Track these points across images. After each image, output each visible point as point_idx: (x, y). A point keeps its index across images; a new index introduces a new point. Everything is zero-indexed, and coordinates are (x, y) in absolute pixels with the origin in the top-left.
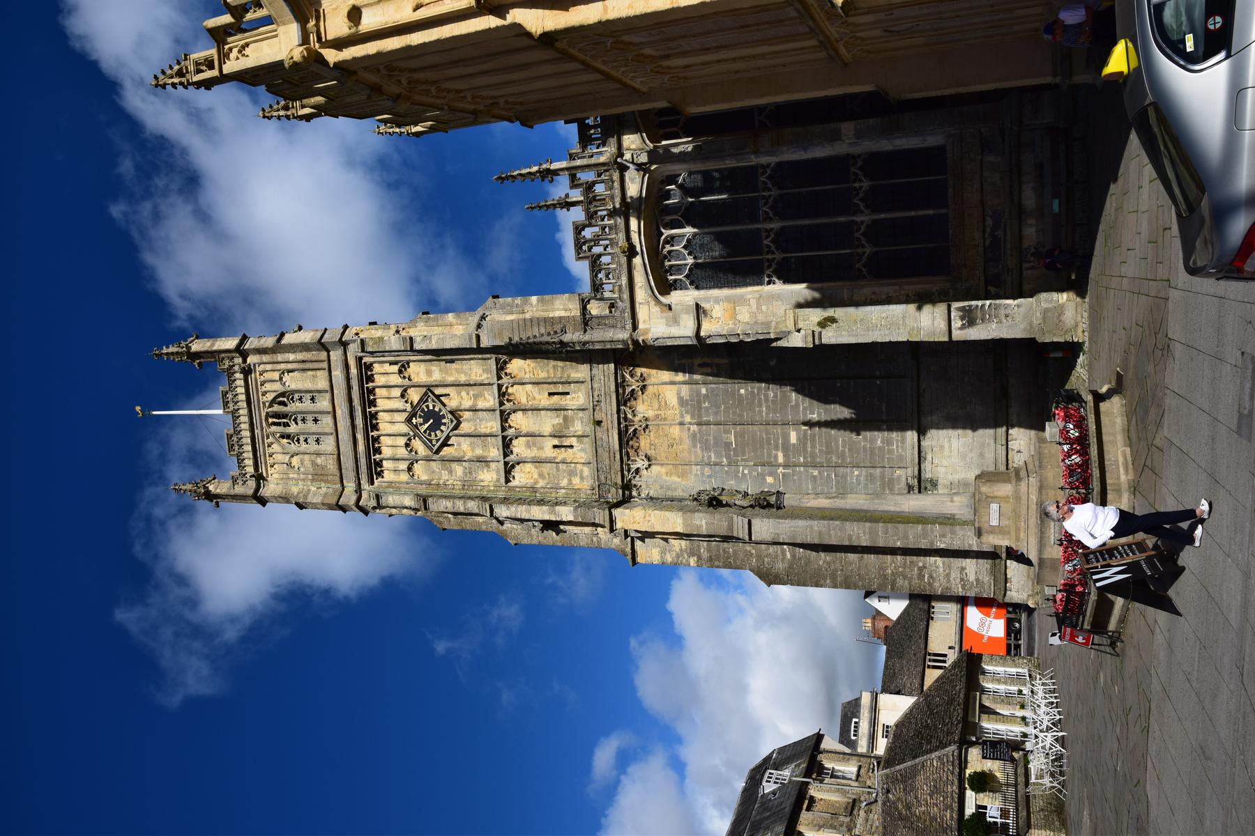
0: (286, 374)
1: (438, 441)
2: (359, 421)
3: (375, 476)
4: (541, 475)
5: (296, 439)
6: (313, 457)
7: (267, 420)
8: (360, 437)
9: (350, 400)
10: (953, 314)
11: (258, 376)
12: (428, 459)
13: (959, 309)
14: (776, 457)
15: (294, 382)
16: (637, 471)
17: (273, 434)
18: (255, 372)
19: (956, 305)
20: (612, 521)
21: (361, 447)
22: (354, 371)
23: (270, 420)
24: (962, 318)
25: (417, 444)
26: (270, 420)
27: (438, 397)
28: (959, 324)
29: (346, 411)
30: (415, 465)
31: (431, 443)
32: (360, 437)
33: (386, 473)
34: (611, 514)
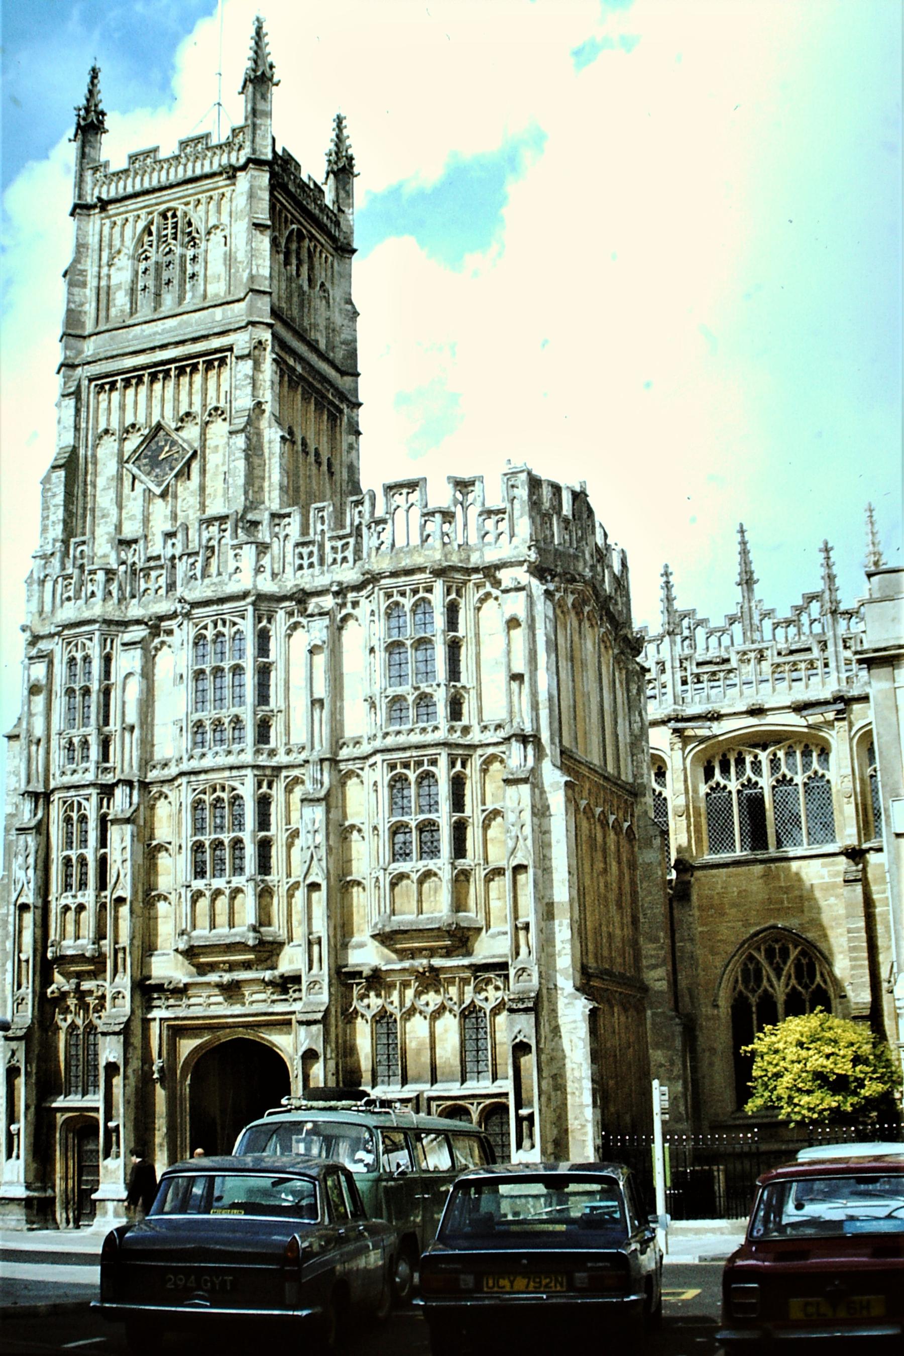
0: (223, 233)
1: (139, 468)
3: (99, 382)
5: (148, 254)
6: (127, 286)
7: (168, 210)
11: (221, 191)
12: (121, 453)
15: (214, 249)
17: (152, 223)
18: (227, 186)
22: (216, 343)
23: (169, 214)
25: (134, 441)
26: (169, 214)
27: (188, 464)
30: (113, 437)
31: (138, 459)
33: (103, 396)
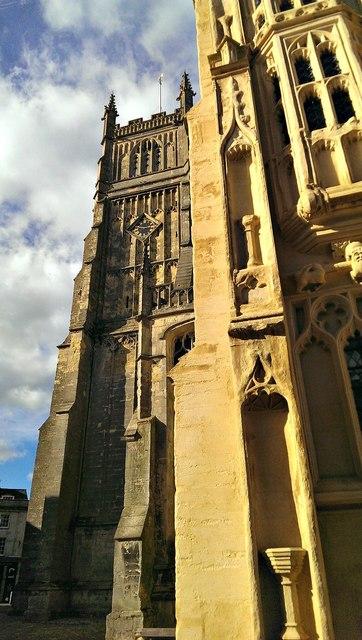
2: (144, 188)
4: (111, 291)
8: (136, 189)
9: (155, 182)
10: (134, 542)
13: (137, 547)
14: (113, 428)
16: (109, 345)
19: (140, 543)
20: (76, 330)
21: (130, 191)
22: (172, 181)
24: (130, 550)
28: (127, 548)
29: (151, 180)
32: (136, 189)
34: (80, 329)
